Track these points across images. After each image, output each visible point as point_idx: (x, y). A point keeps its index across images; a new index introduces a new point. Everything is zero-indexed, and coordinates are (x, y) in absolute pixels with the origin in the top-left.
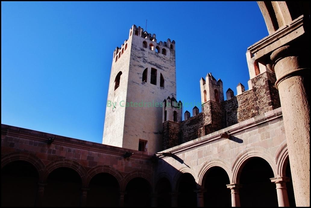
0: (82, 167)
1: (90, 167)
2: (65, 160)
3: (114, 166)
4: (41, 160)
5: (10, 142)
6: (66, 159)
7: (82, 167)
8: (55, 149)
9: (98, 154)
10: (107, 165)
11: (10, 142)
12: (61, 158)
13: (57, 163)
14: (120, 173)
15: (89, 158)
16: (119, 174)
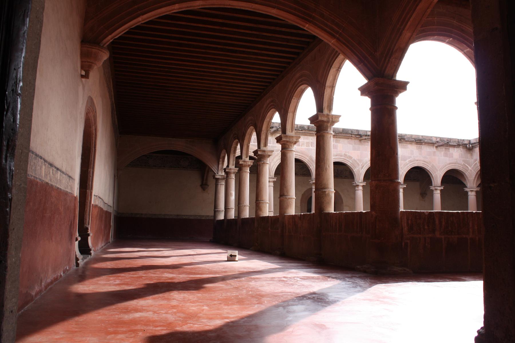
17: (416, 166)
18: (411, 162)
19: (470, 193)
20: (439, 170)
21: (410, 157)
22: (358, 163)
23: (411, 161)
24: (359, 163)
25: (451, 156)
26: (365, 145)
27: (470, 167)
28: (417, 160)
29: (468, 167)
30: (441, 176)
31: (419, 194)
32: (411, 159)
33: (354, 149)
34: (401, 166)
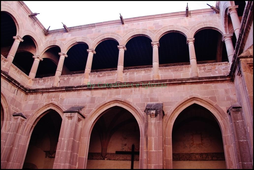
0: (150, 31)
1: (157, 29)
2: (136, 30)
3: (178, 24)
4: (119, 34)
5: (98, 30)
6: (136, 29)
7: (150, 31)
8: (127, 26)
9: (162, 20)
10: (171, 24)
11: (98, 30)
12: (133, 30)
13: (130, 33)
14: (185, 28)
15: (154, 24)
16: (184, 28)
19: (36, 59)
25: (35, 29)
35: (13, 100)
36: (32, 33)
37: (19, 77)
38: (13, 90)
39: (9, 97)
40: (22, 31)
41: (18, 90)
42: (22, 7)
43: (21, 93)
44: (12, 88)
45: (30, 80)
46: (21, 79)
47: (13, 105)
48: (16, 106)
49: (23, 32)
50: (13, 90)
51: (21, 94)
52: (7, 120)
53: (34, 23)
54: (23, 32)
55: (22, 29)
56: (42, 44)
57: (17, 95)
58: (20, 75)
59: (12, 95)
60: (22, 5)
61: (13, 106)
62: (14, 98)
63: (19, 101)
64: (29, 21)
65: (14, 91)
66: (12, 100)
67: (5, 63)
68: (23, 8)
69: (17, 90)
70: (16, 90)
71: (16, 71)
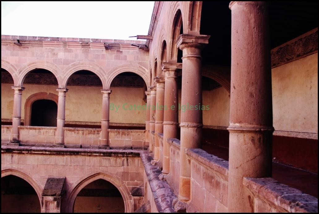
17: (81, 69)
18: (74, 66)
20: (107, 73)
21: (73, 61)
22: (16, 69)
23: (74, 65)
24: (17, 69)
25: (125, 58)
26: (25, 51)
27: (148, 69)
28: (82, 64)
29: (144, 70)
30: (111, 79)
31: (142, 99)
32: (75, 63)
33: (12, 55)
34: (63, 70)
35: (125, 175)
36: (122, 66)
37: (128, 139)
38: (120, 162)
39: (117, 174)
40: (104, 78)
41: (127, 160)
42: (90, 48)
43: (135, 160)
44: (117, 162)
45: (146, 133)
46: (131, 139)
47: (128, 180)
48: (132, 179)
49: (106, 78)
50: (120, 162)
51: (133, 161)
52: (127, 200)
53: (119, 52)
54: (106, 79)
55: (103, 76)
56: (146, 69)
57: (128, 165)
58: (128, 135)
59: (121, 170)
60: (89, 45)
61: (127, 182)
62: (126, 171)
63: (134, 172)
64: (110, 56)
65: (121, 162)
66: (122, 176)
67: (100, 134)
68: (92, 48)
69: (126, 160)
70: (124, 160)
71: (120, 134)
